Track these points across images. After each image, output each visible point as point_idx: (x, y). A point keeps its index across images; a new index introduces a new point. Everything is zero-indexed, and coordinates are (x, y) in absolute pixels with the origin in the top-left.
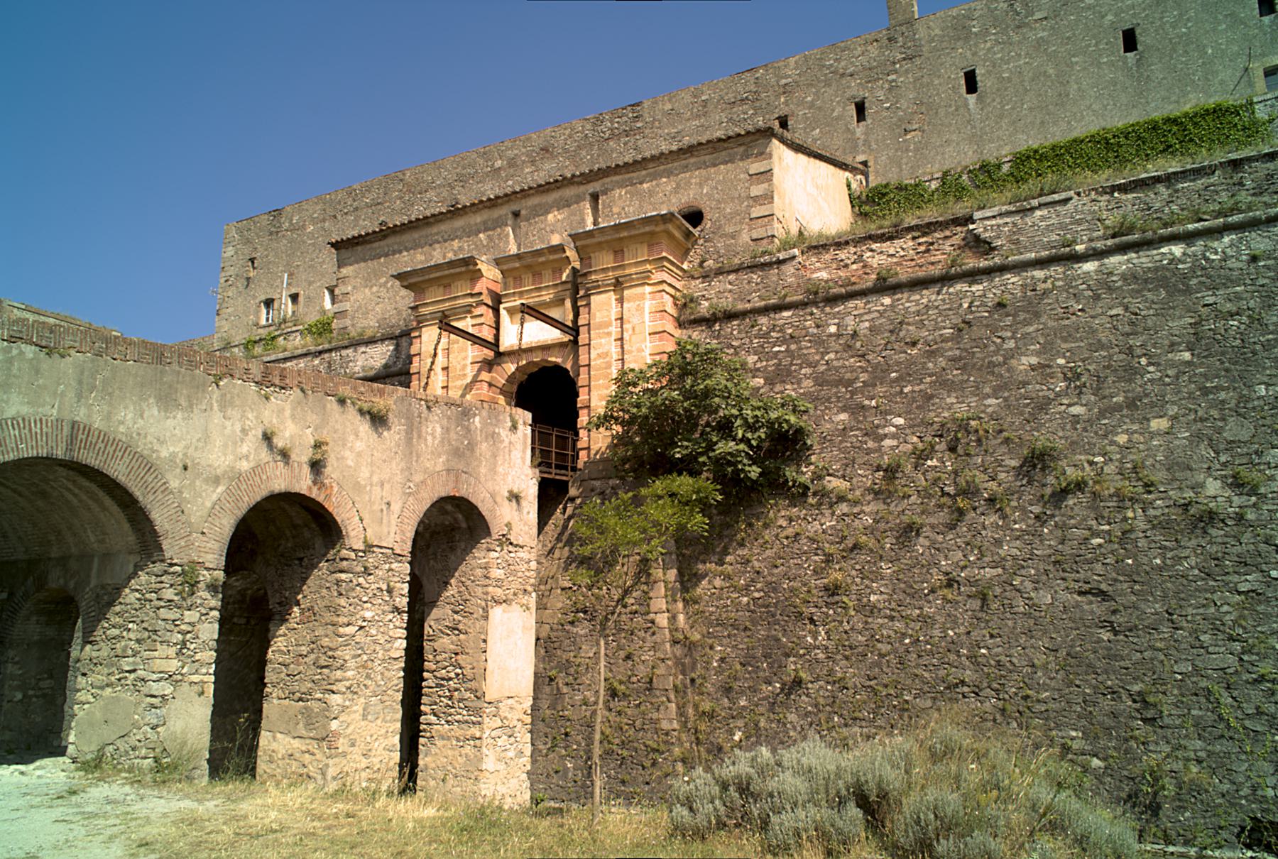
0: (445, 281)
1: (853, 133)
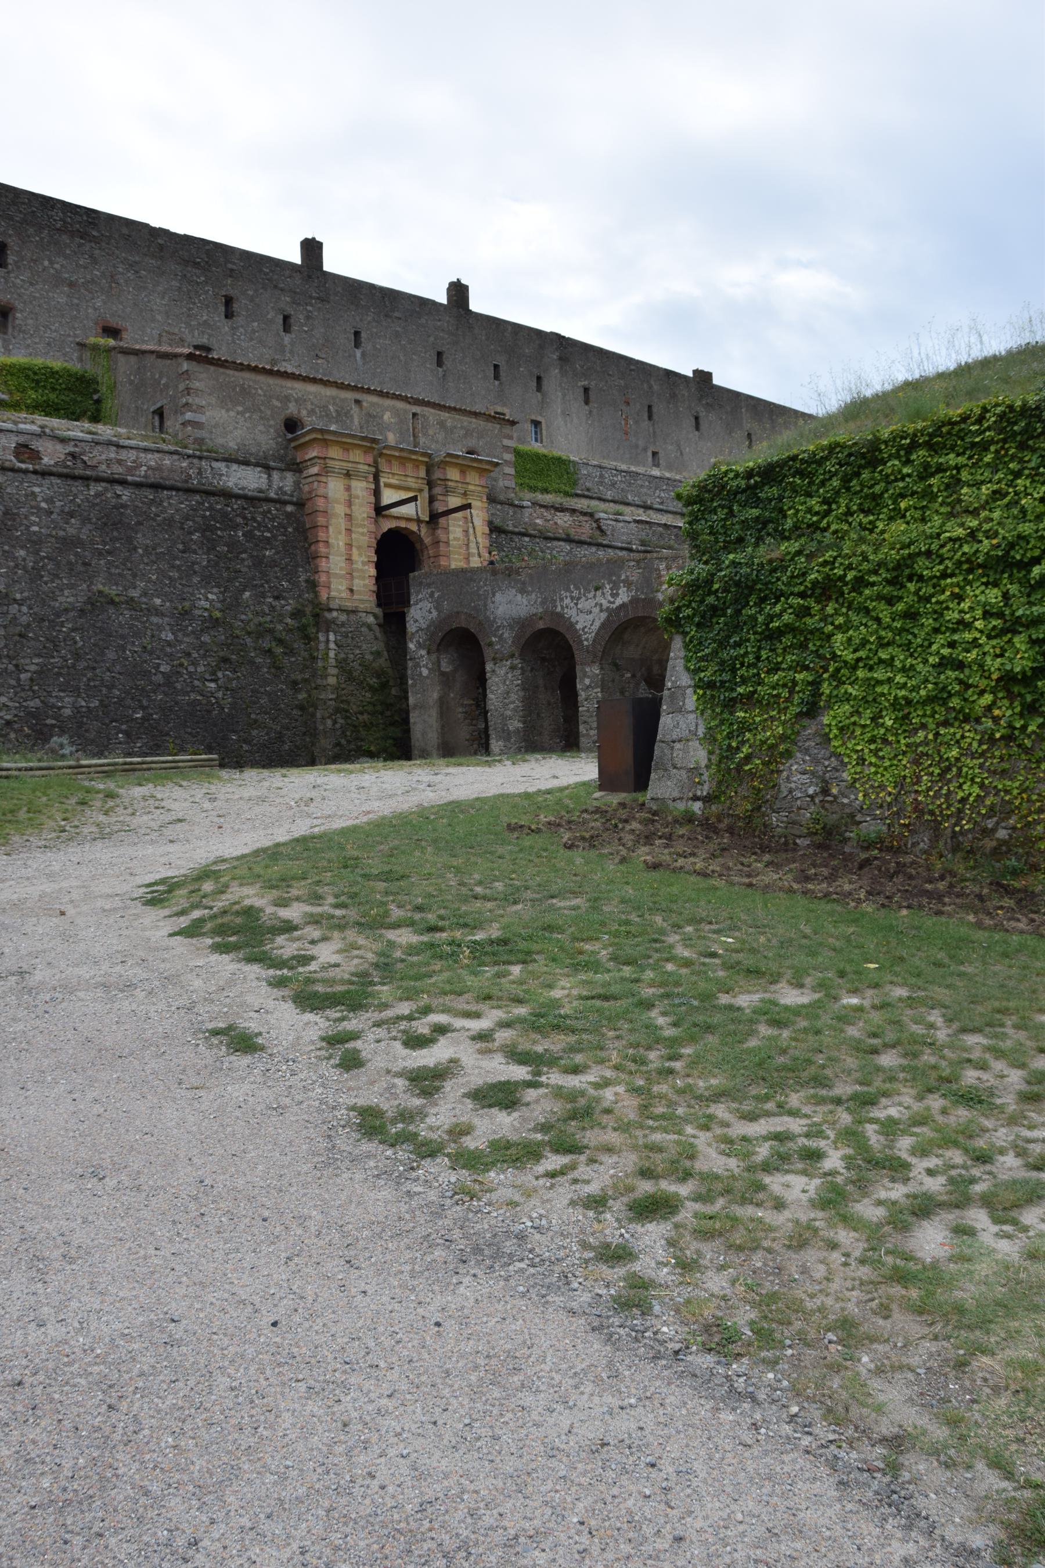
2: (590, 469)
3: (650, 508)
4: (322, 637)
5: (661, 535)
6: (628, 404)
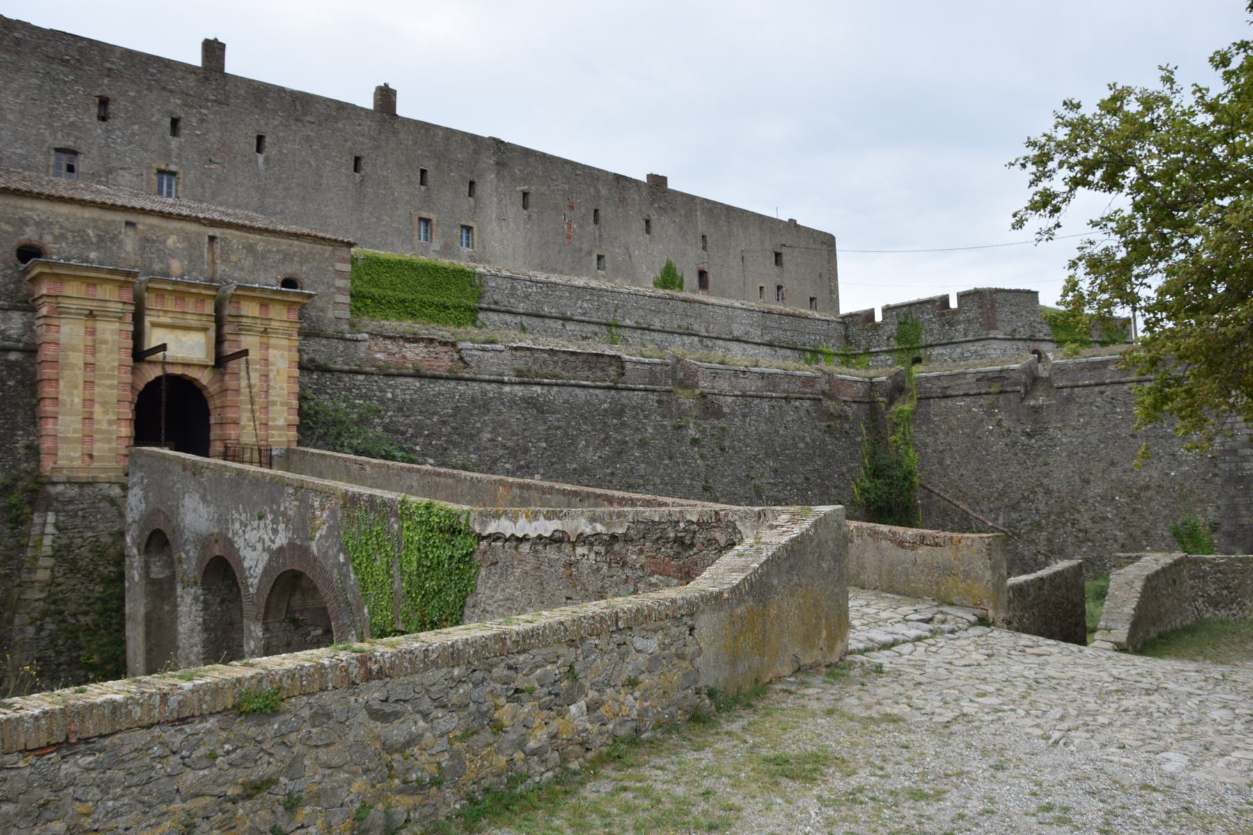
1: (169, 144)
2: (499, 281)
3: (570, 319)
4: (37, 519)
5: (545, 362)
6: (572, 208)
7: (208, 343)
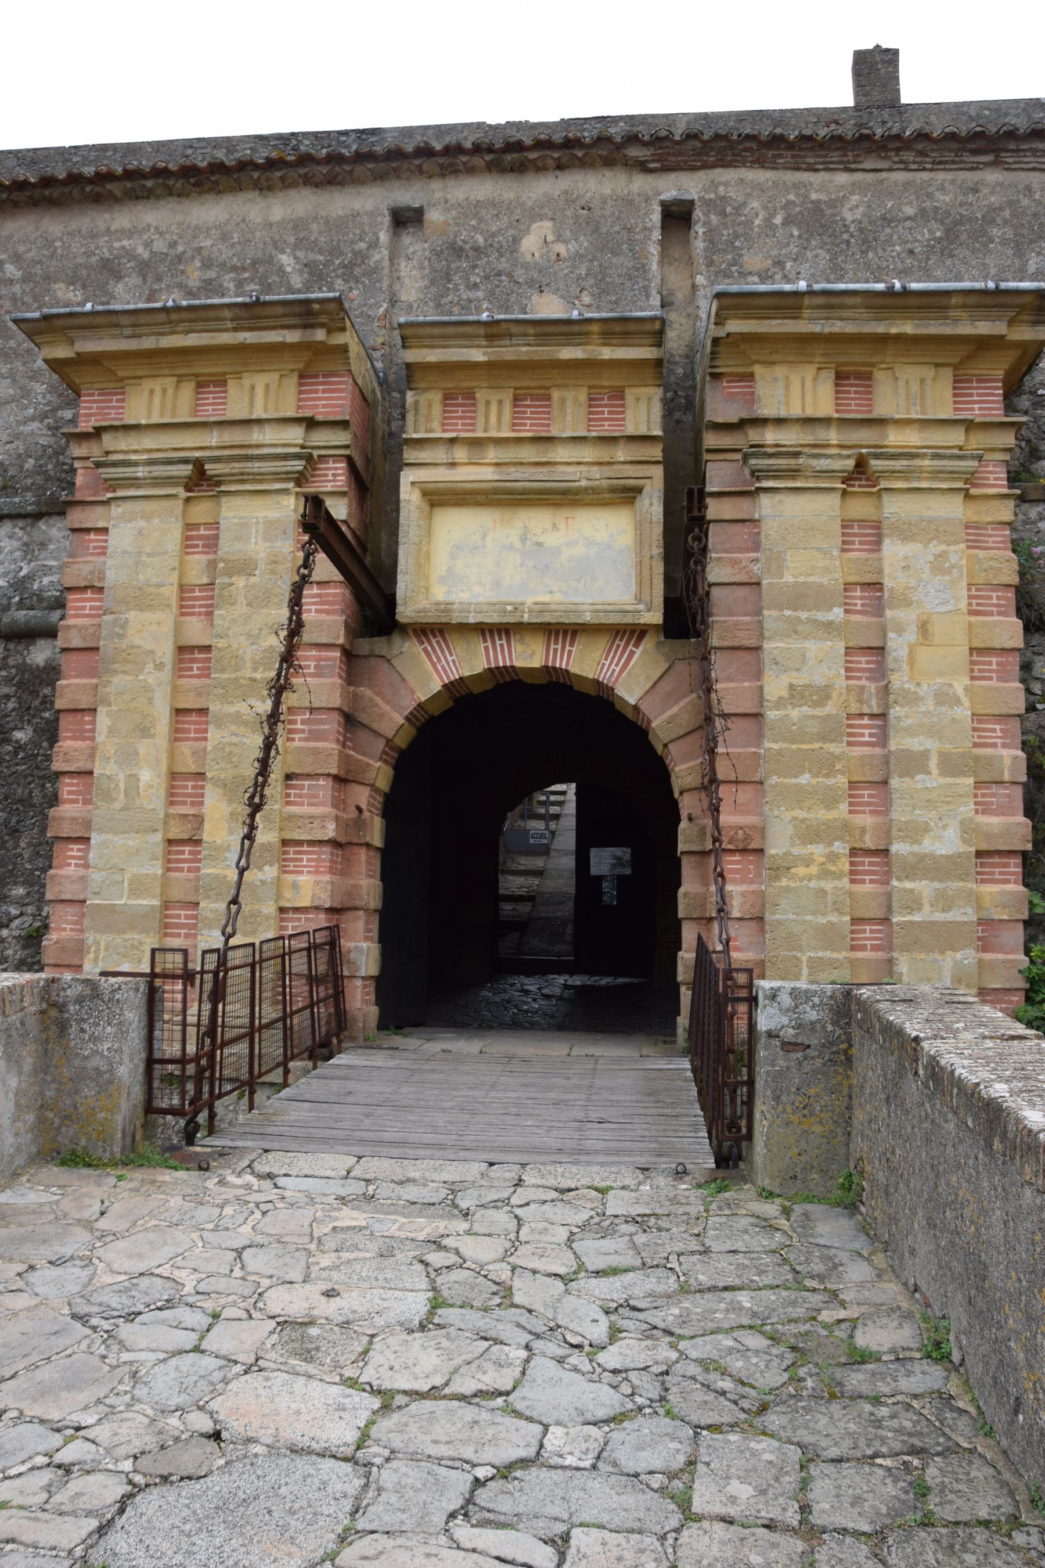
0: (206, 368)
7: (640, 543)
